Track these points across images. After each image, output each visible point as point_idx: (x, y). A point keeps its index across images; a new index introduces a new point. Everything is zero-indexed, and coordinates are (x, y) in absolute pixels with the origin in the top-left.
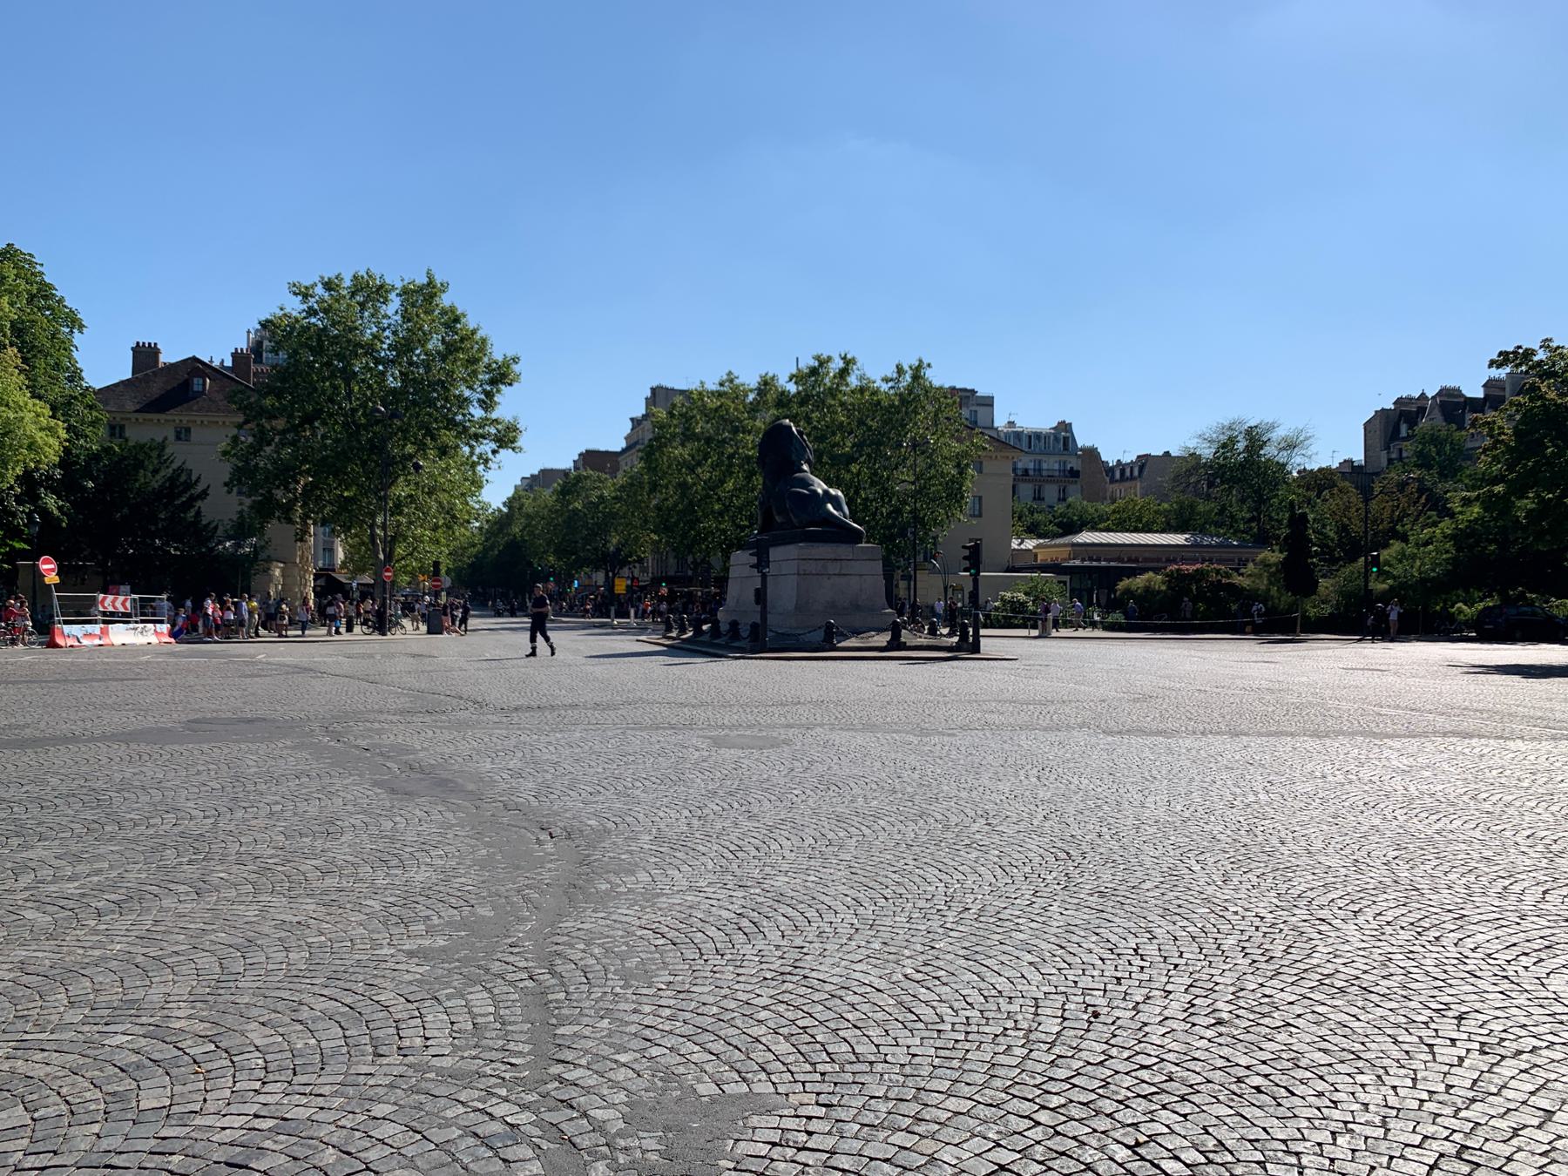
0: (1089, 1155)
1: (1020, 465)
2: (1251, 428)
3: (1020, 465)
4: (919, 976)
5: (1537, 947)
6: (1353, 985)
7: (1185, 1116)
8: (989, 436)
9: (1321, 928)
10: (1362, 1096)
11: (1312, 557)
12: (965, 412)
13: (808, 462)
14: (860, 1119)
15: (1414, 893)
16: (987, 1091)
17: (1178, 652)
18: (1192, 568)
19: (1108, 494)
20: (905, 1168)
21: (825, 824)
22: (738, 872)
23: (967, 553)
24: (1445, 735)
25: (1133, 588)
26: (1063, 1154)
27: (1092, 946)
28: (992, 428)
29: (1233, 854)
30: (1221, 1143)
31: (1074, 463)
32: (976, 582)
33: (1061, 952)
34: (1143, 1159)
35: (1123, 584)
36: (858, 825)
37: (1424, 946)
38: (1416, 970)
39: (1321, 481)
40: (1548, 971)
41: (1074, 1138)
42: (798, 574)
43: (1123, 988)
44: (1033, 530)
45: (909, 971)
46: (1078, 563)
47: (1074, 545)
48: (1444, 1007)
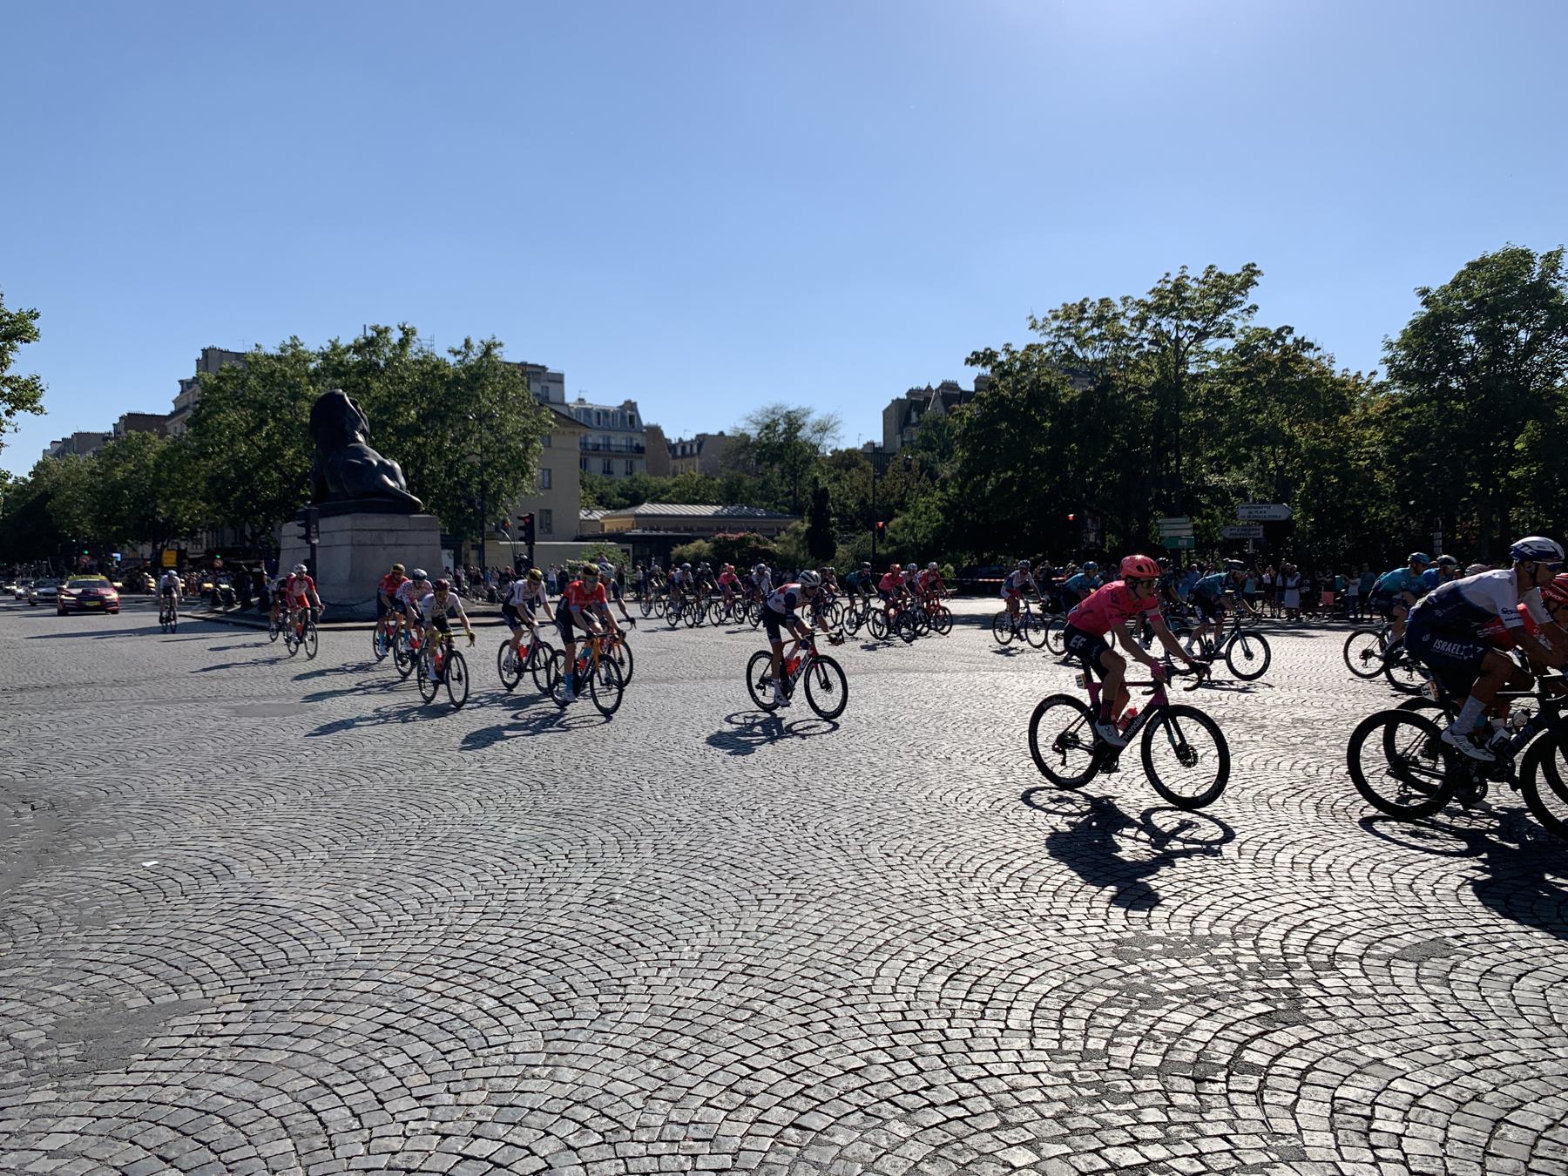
0: (460, 1009)
1: (590, 440)
3: (590, 440)
4: (370, 894)
7: (551, 972)
8: (556, 412)
10: (694, 941)
12: (536, 387)
13: (363, 432)
14: (276, 1007)
16: (395, 974)
19: (671, 469)
20: (302, 1038)
21: (327, 779)
22: (225, 826)
23: (522, 523)
24: (891, 671)
25: (685, 554)
26: (442, 1010)
27: (531, 855)
28: (563, 404)
30: (571, 986)
31: (639, 440)
32: (531, 550)
33: (503, 863)
34: (505, 1005)
35: (678, 550)
36: (358, 777)
39: (846, 460)
41: (455, 998)
42: (353, 545)
43: (543, 885)
44: (602, 501)
45: (361, 891)
46: (639, 532)
47: (637, 516)
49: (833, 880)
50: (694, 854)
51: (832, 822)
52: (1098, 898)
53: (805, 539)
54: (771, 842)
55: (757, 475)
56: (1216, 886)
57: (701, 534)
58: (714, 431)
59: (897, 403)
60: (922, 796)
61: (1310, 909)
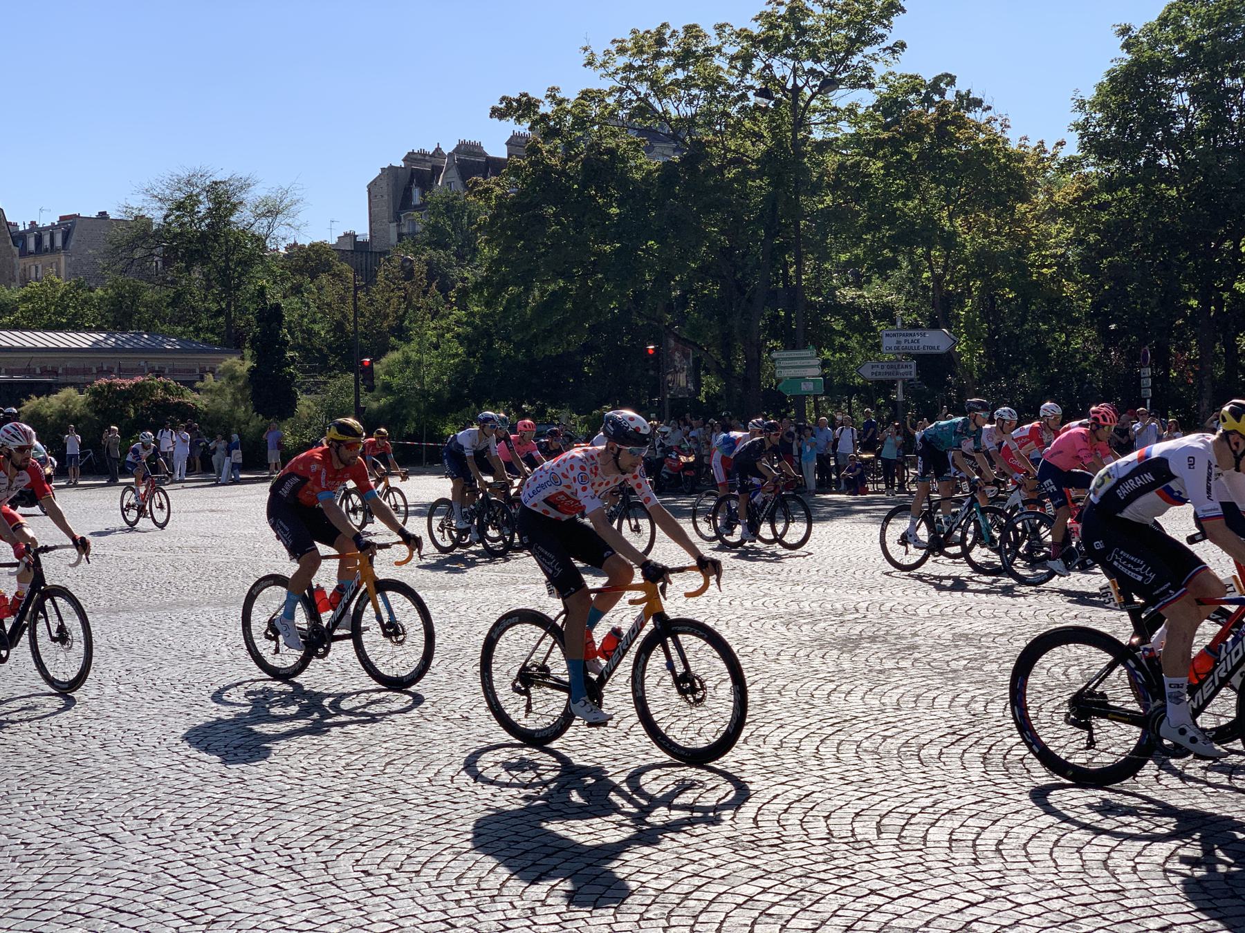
2: (216, 183)
5: (344, 827)
6: (103, 907)
9: (100, 846)
11: (289, 365)
15: (238, 786)
17: (96, 503)
18: (128, 382)
19: (18, 273)
25: (45, 411)
29: (31, 768)
37: (213, 848)
38: (192, 876)
40: (339, 852)
48: (200, 913)
49: (278, 919)
50: (50, 895)
51: (280, 830)
52: (679, 911)
53: (245, 387)
54: (180, 868)
55: (164, 283)
56: (847, 882)
57: (70, 379)
58: (89, 211)
59: (390, 172)
60: (423, 778)
61: (972, 905)
